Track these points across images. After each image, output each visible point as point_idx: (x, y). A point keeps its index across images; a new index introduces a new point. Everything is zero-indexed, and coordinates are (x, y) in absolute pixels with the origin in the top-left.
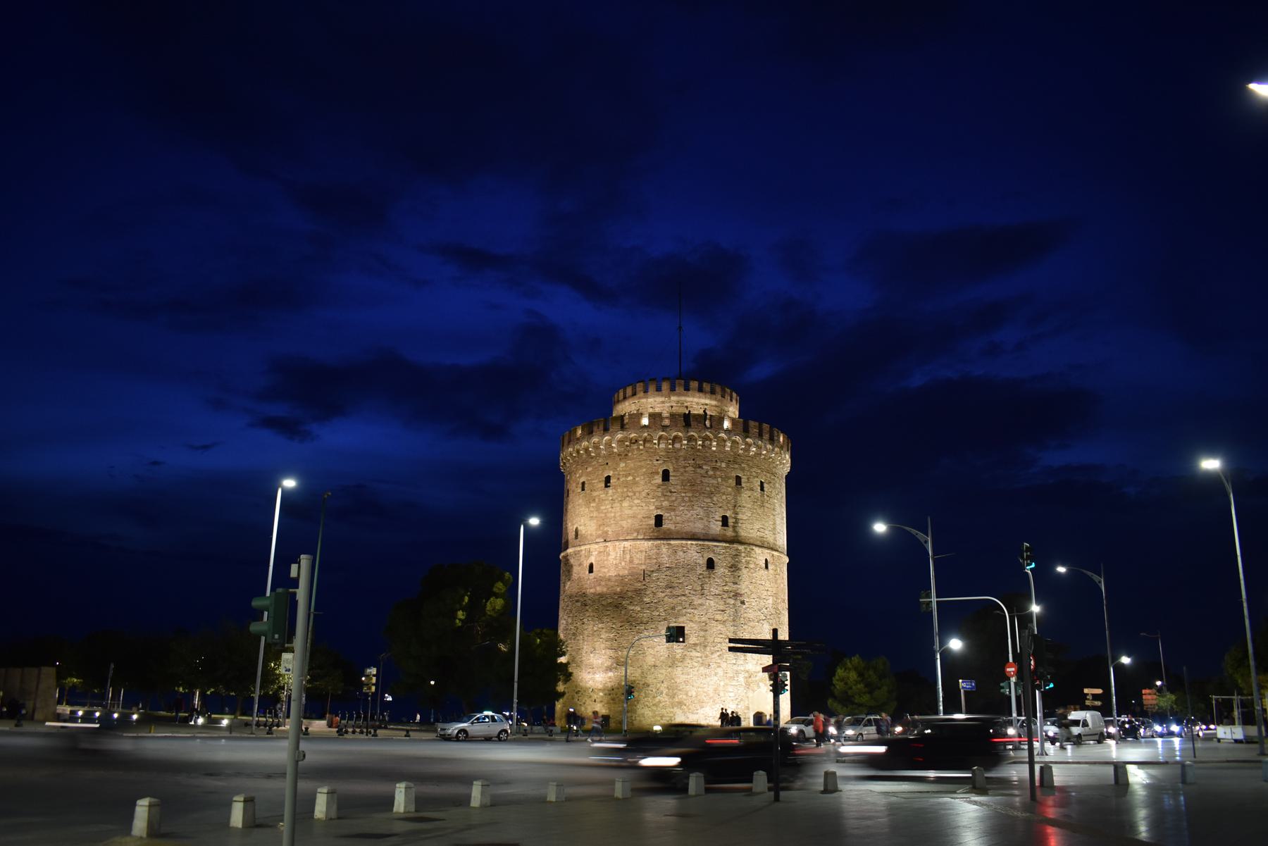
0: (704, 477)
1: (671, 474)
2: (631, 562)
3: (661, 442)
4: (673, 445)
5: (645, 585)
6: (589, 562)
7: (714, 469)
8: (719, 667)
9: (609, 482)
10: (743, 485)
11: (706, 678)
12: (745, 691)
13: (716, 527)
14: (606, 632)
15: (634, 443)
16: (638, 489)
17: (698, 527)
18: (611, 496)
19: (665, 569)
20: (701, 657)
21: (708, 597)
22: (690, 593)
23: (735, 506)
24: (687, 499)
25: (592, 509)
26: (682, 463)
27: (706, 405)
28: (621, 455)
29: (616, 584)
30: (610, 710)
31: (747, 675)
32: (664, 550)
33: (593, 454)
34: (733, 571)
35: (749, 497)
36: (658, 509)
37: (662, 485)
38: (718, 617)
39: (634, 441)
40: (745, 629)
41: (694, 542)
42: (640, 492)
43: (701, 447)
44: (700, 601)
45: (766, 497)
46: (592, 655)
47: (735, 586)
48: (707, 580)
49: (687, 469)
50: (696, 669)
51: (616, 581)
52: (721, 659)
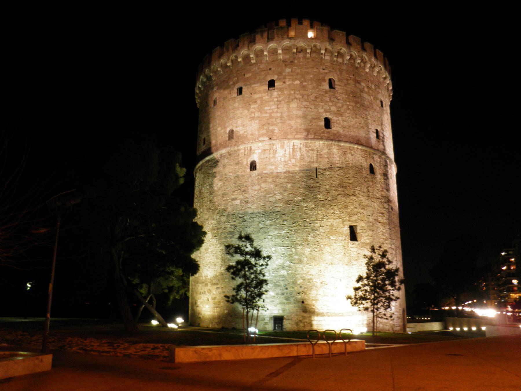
1: (336, 83)
5: (317, 183)
6: (250, 160)
7: (368, 87)
14: (276, 229)
15: (300, 52)
18: (277, 98)
22: (359, 194)
24: (351, 107)
25: (253, 110)
28: (286, 62)
29: (286, 180)
32: (335, 150)
37: (330, 92)
39: (299, 50)
41: (360, 147)
42: (308, 96)
47: (387, 193)
49: (349, 82)
51: (286, 178)
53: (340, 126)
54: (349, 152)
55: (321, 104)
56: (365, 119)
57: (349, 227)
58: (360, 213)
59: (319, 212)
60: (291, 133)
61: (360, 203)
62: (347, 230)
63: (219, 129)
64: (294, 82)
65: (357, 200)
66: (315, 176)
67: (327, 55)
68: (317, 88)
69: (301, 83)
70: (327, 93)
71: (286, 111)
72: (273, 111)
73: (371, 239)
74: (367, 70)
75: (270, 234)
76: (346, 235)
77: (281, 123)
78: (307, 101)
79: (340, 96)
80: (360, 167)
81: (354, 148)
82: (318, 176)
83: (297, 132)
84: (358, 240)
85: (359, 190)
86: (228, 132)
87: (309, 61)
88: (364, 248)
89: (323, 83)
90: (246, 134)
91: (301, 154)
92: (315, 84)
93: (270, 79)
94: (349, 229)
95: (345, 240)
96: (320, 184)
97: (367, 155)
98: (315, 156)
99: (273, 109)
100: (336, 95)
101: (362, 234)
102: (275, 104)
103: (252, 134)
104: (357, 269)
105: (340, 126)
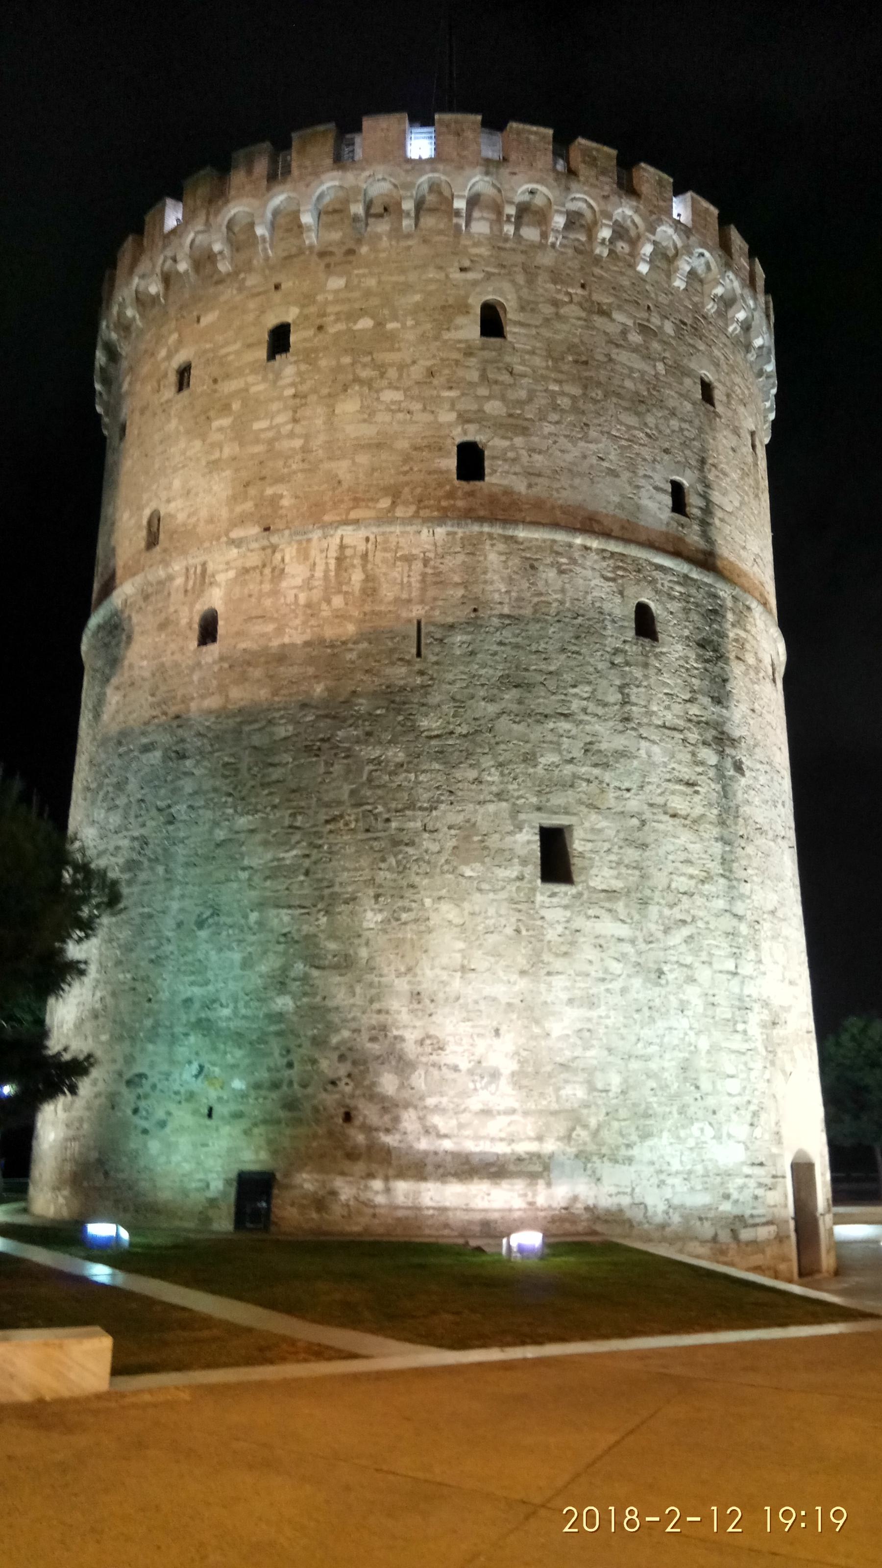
0: (618, 346)
1: (510, 316)
2: (370, 589)
3: (476, 214)
5: (421, 673)
6: (200, 608)
7: (644, 329)
8: (691, 980)
11: (652, 1020)
12: (767, 1076)
14: (266, 843)
15: (380, 216)
19: (496, 621)
21: (644, 732)
26: (545, 286)
28: (331, 253)
29: (311, 671)
30: (275, 1153)
32: (493, 557)
36: (469, 421)
37: (483, 349)
38: (678, 804)
39: (377, 209)
40: (749, 856)
41: (595, 544)
44: (620, 742)
46: (203, 934)
47: (716, 709)
48: (638, 673)
50: (616, 986)
51: (311, 660)
52: (696, 953)
53: (517, 469)
54: (549, 560)
55: (446, 394)
56: (624, 443)
57: (537, 831)
58: (589, 781)
59: (422, 778)
60: (336, 505)
61: (591, 743)
62: (529, 842)
63: (126, 515)
64: (355, 323)
65: (574, 732)
66: (414, 651)
67: (482, 218)
68: (436, 338)
69: (380, 324)
71: (323, 427)
72: (279, 432)
73: (632, 875)
74: (643, 268)
75: (246, 862)
76: (524, 862)
77: (302, 471)
78: (397, 388)
79: (523, 363)
80: (592, 614)
81: (570, 546)
82: (424, 651)
83: (355, 499)
84: (576, 878)
85: (586, 695)
86: (145, 522)
87: (410, 243)
88: (603, 911)
89: (460, 320)
90: (193, 520)
91: (367, 576)
92: (429, 326)
94: (538, 837)
95: (521, 878)
96: (432, 679)
97: (625, 569)
98: (415, 580)
99: (278, 426)
100: (508, 359)
101: (590, 859)
102: (285, 408)
103: (211, 521)
104: (566, 989)
105: (517, 469)
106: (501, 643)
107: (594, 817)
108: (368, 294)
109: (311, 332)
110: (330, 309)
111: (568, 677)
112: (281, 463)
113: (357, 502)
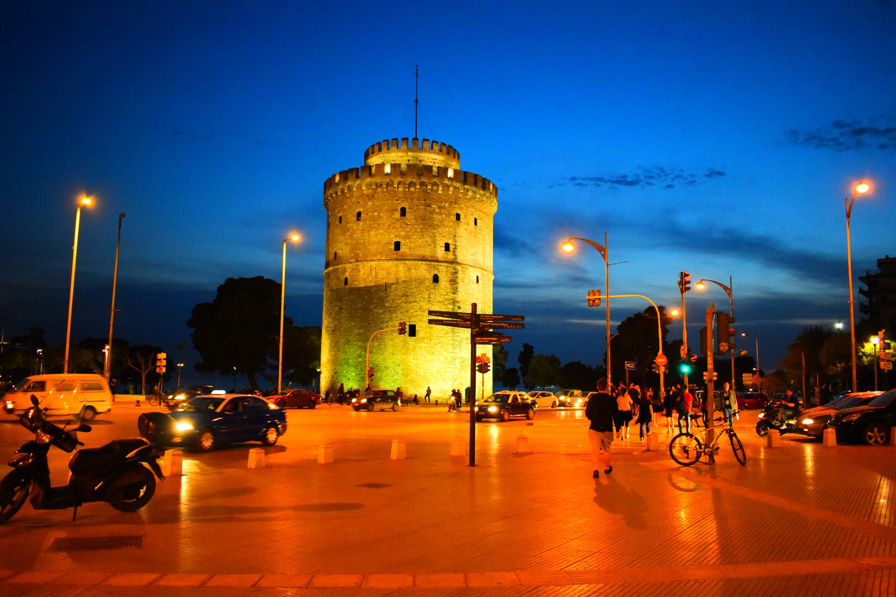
1: (407, 211)
3: (400, 186)
4: (409, 189)
5: (386, 294)
7: (440, 208)
9: (360, 217)
10: (461, 220)
12: (460, 372)
13: (440, 253)
14: (357, 329)
15: (379, 187)
16: (381, 222)
17: (427, 252)
20: (428, 347)
22: (420, 300)
23: (455, 236)
24: (419, 230)
25: (347, 237)
27: (435, 159)
30: (360, 386)
31: (461, 360)
33: (348, 195)
34: (453, 284)
35: (466, 229)
36: (397, 237)
37: (401, 219)
39: (379, 185)
41: (424, 263)
42: (383, 224)
43: (430, 191)
45: (478, 230)
46: (346, 346)
47: (454, 295)
48: (433, 291)
49: (419, 208)
50: (424, 355)
53: (407, 247)
68: (391, 217)
69: (379, 214)
70: (397, 221)
79: (409, 222)
80: (422, 279)
87: (385, 194)
89: (396, 213)
92: (389, 214)
93: (357, 211)
105: (407, 247)
106: (402, 287)
107: (420, 322)
108: (377, 206)
109: (365, 215)
110: (369, 210)
111: (416, 293)
112: (359, 245)
113: (373, 257)
